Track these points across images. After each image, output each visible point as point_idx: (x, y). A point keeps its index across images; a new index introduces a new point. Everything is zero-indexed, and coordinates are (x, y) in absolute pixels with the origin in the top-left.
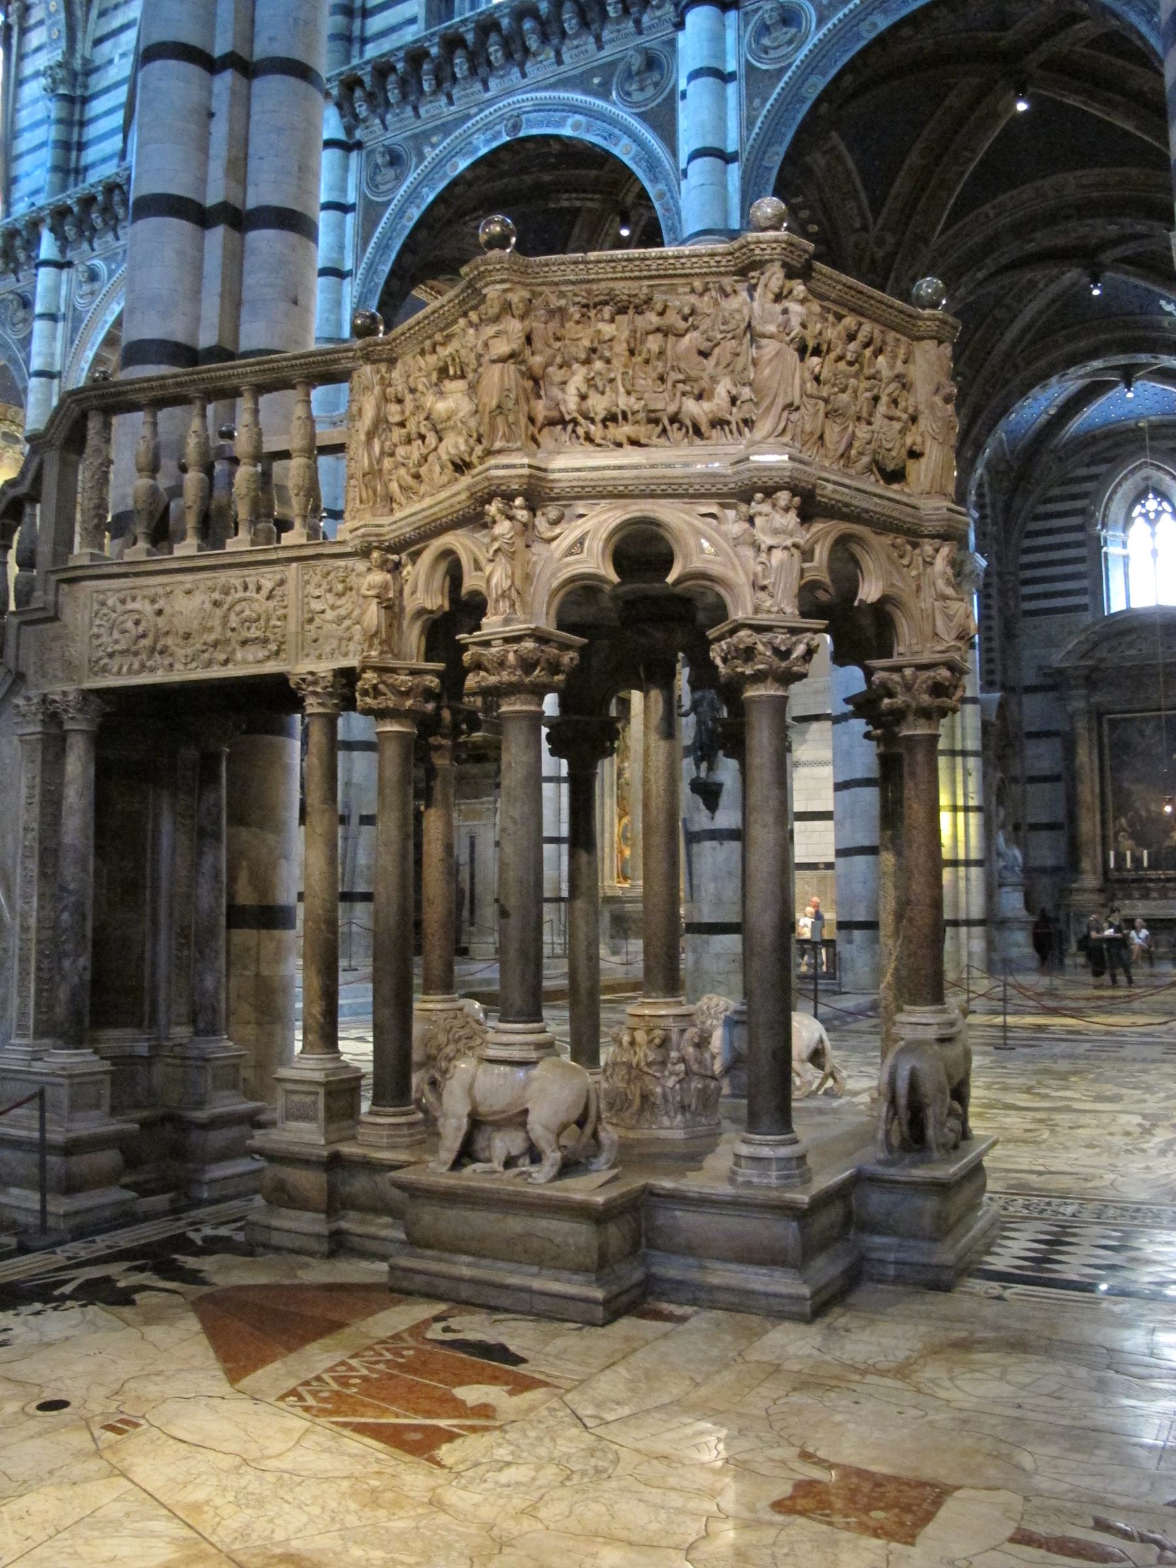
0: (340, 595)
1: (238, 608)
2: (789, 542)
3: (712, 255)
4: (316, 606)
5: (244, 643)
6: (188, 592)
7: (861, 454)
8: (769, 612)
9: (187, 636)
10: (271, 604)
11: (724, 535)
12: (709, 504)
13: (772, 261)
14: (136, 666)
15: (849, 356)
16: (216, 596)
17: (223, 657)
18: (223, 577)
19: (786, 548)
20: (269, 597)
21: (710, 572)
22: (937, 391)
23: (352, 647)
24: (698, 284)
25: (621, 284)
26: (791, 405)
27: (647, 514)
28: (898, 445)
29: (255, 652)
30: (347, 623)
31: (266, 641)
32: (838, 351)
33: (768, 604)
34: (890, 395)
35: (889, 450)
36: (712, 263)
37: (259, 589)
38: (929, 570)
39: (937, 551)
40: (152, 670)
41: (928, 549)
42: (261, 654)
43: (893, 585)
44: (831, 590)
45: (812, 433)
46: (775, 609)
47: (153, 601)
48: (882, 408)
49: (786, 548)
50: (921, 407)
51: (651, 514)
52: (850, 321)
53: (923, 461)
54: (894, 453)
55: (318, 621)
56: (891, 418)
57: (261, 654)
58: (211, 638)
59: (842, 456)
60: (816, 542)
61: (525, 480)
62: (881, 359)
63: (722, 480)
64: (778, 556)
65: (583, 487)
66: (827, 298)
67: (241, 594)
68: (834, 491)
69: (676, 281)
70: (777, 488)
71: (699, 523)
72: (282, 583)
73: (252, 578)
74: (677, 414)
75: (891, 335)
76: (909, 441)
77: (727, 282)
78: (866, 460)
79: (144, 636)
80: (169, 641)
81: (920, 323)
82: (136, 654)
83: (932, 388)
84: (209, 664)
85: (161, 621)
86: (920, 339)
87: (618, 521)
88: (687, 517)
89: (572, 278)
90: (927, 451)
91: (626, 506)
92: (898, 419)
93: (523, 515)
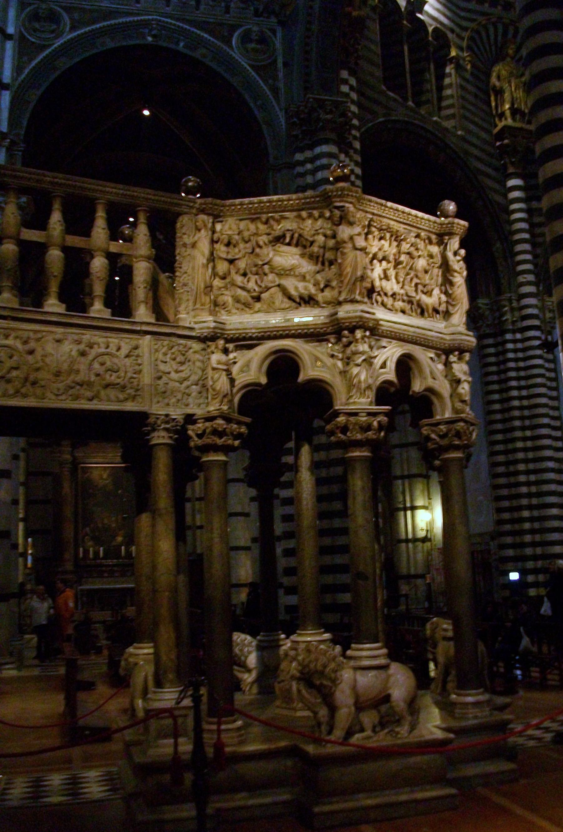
0: (182, 363)
1: (100, 359)
4: (162, 367)
5: (107, 386)
6: (58, 341)
9: (58, 374)
10: (128, 361)
14: (11, 391)
16: (82, 347)
17: (89, 394)
18: (88, 336)
20: (127, 356)
23: (190, 400)
29: (112, 393)
30: (186, 383)
31: (124, 387)
37: (119, 349)
40: (25, 396)
42: (121, 396)
47: (25, 342)
55: (165, 379)
57: (121, 396)
58: (78, 378)
67: (103, 350)
72: (136, 348)
73: (114, 340)
79: (16, 368)
80: (40, 375)
82: (9, 381)
84: (77, 398)
85: (30, 358)
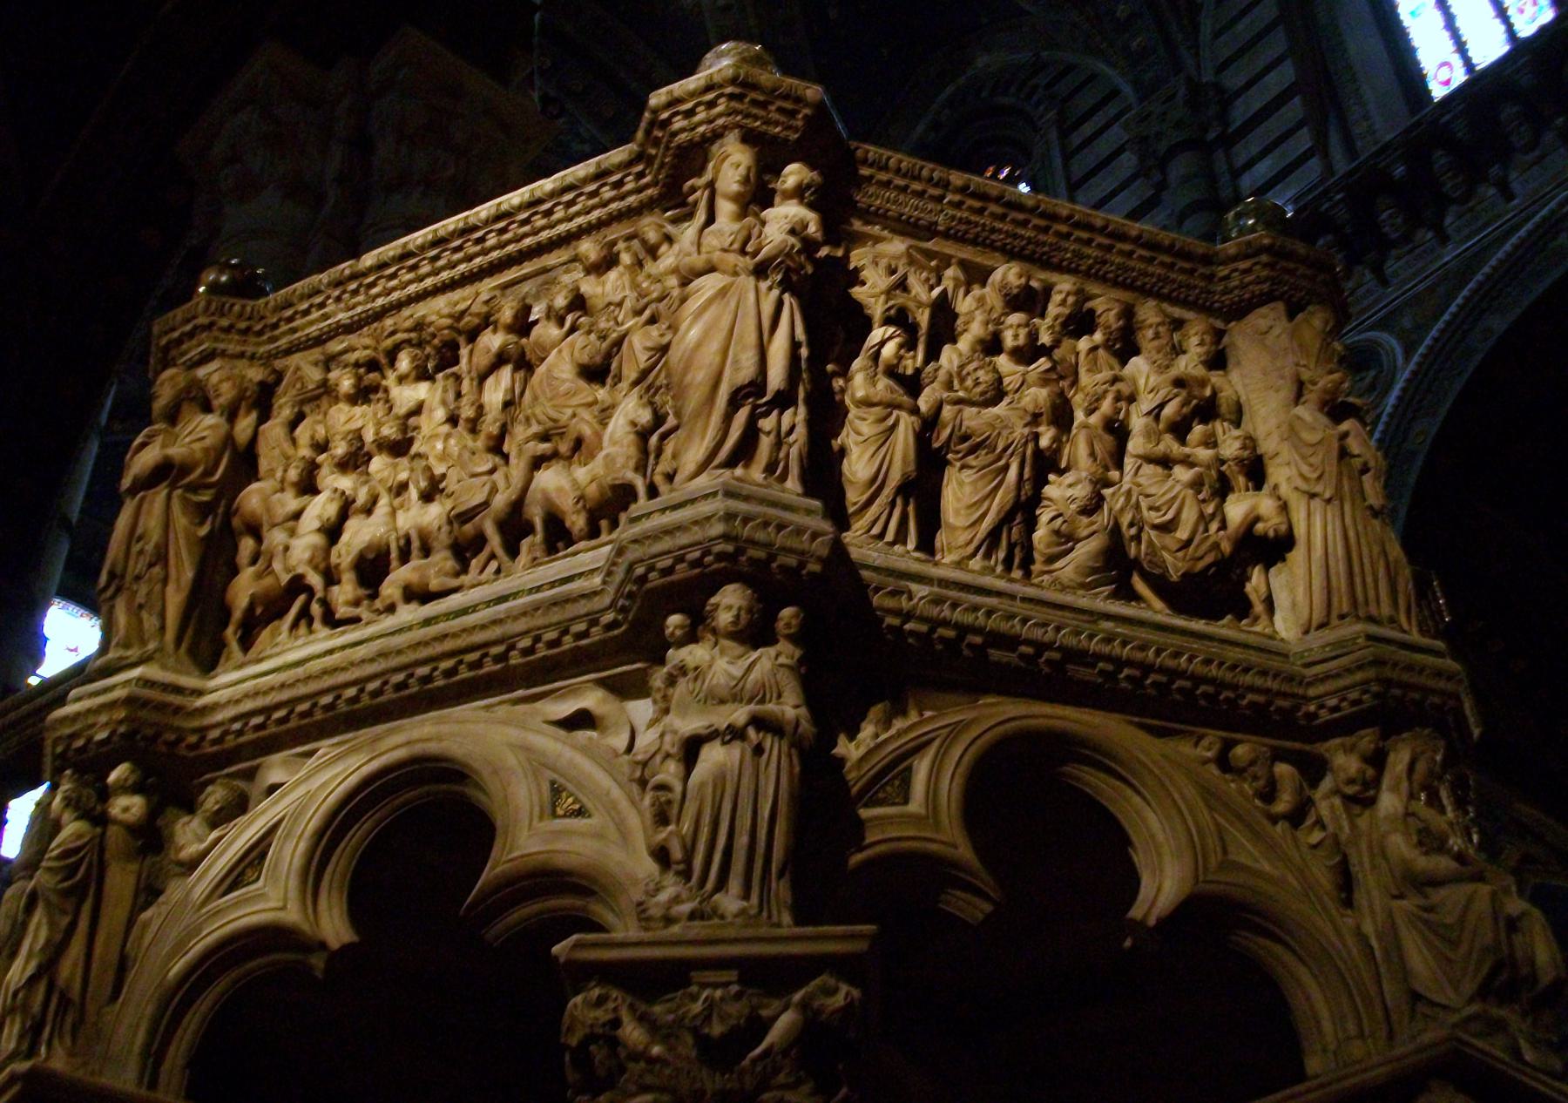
2: (739, 714)
3: (600, 175)
7: (1066, 539)
8: (669, 920)
11: (607, 761)
12: (573, 691)
13: (717, 135)
15: (1009, 340)
19: (734, 734)
21: (561, 862)
22: (1298, 397)
24: (589, 248)
25: (441, 303)
26: (756, 386)
27: (418, 749)
28: (1189, 516)
32: (973, 331)
33: (663, 897)
34: (1156, 413)
35: (1167, 528)
36: (607, 193)
38: (1363, 822)
39: (1377, 760)
41: (1345, 762)
43: (1227, 865)
44: (985, 880)
45: (876, 483)
46: (686, 908)
48: (1135, 445)
49: (734, 734)
50: (1267, 446)
51: (433, 748)
52: (1008, 274)
53: (1297, 556)
54: (1183, 534)
56: (1166, 462)
59: (993, 537)
60: (919, 749)
61: (121, 714)
62: (1136, 362)
63: (583, 607)
64: (713, 756)
65: (267, 711)
66: (930, 231)
68: (938, 601)
69: (550, 259)
70: (714, 583)
71: (555, 745)
74: (518, 505)
75: (1148, 312)
76: (1236, 509)
77: (649, 227)
78: (1085, 551)
81: (1223, 271)
83: (1287, 391)
86: (1239, 311)
87: (353, 780)
88: (513, 733)
89: (343, 316)
90: (1300, 531)
91: (377, 739)
92: (1188, 462)
93: (126, 807)
